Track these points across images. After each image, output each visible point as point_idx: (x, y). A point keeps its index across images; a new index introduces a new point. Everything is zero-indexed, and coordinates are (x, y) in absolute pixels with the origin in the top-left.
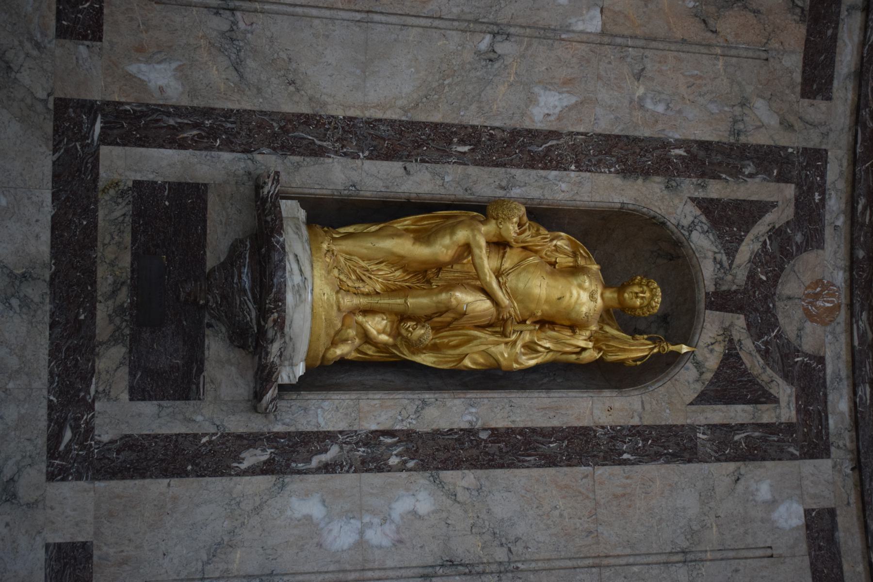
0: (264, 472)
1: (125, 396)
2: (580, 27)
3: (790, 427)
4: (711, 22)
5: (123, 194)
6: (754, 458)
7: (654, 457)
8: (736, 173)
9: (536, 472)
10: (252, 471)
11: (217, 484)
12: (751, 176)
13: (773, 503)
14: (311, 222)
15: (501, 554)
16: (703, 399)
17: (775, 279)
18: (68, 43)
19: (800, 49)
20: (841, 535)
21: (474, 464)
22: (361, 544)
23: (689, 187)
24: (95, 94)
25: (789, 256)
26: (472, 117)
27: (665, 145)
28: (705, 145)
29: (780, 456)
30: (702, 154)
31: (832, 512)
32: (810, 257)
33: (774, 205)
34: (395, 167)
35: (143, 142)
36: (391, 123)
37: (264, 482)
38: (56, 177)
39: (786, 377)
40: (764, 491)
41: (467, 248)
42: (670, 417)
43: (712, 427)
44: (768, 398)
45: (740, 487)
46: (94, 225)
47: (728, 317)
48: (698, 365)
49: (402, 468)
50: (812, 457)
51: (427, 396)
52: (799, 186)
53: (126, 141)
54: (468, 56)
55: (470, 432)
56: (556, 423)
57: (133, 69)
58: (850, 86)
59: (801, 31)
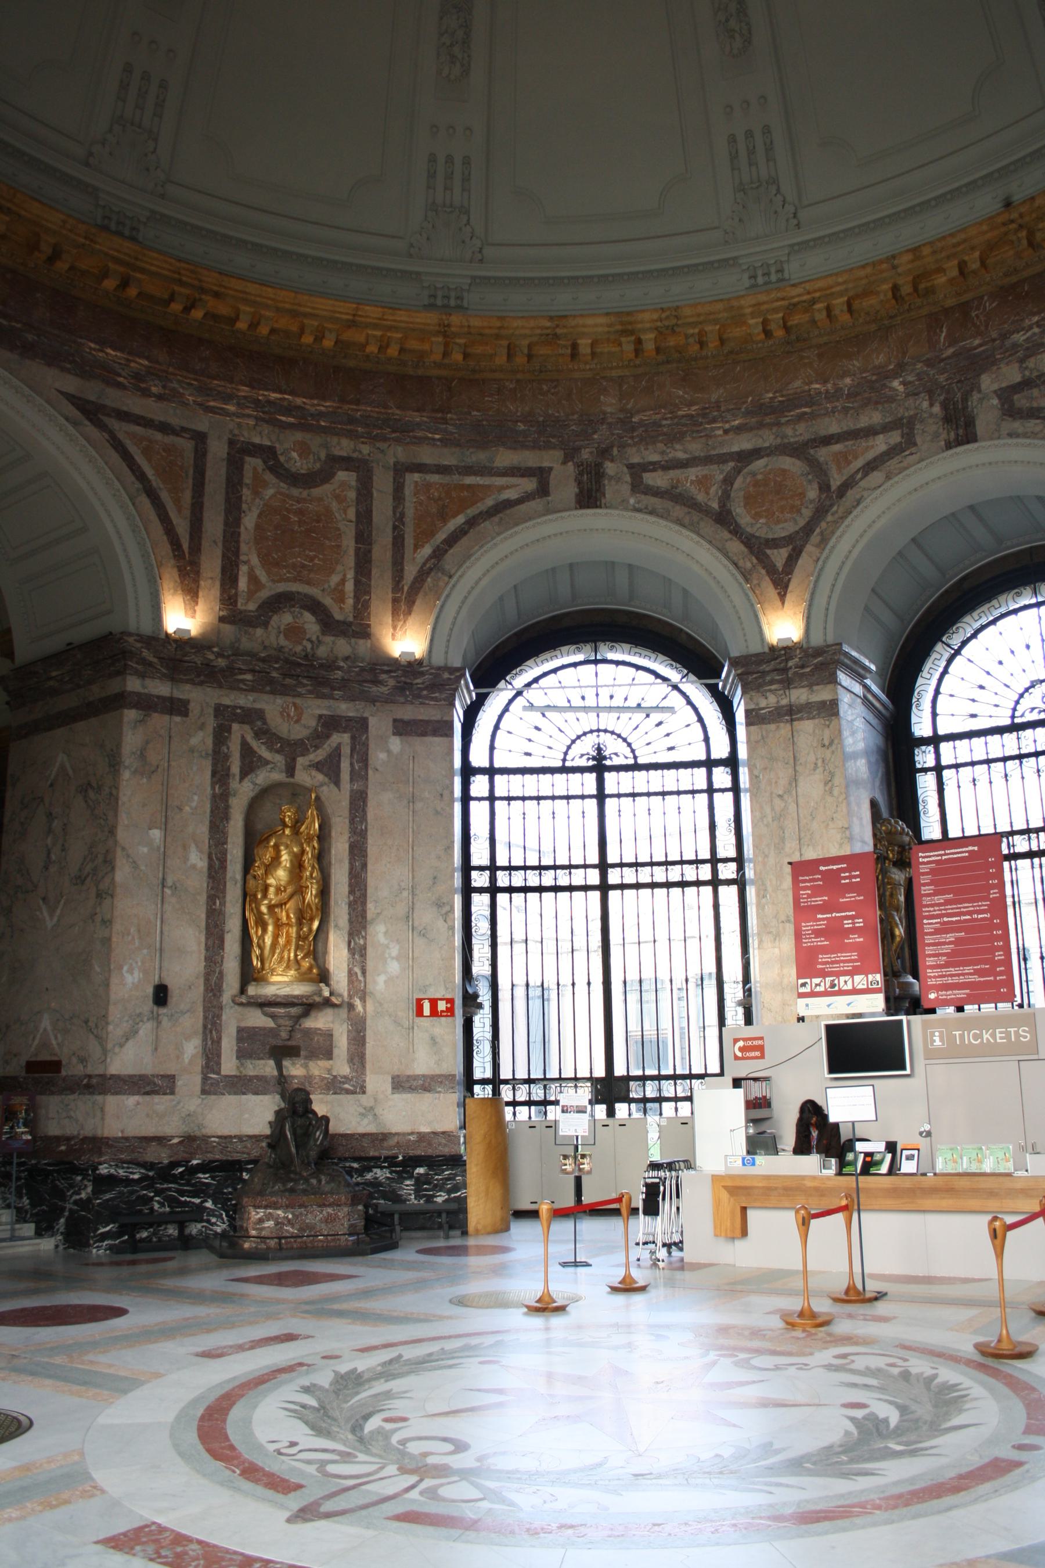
0: (365, 1002)
1: (331, 1062)
2: (158, 841)
3: (353, 738)
4: (153, 769)
5: (242, 1064)
6: (367, 760)
7: (364, 812)
8: (227, 757)
9: (369, 874)
11: (369, 1022)
12: (228, 748)
15: (405, 894)
16: (337, 783)
17: (280, 739)
18: (177, 1090)
20: (406, 717)
21: (364, 903)
22: (397, 958)
23: (234, 784)
24: (198, 1079)
26: (203, 899)
27: (214, 796)
28: (214, 773)
29: (366, 745)
30: (218, 776)
31: (395, 721)
32: (269, 716)
33: (243, 737)
34: (228, 938)
35: (219, 1056)
36: (207, 939)
38: (235, 1093)
39: (328, 737)
40: (383, 756)
42: (345, 803)
43: (352, 780)
44: (338, 748)
46: (256, 1077)
47: (298, 767)
48: (322, 785)
49: (365, 938)
50: (367, 727)
52: (233, 721)
53: (219, 1064)
55: (350, 904)
57: (187, 1061)
59: (155, 715)
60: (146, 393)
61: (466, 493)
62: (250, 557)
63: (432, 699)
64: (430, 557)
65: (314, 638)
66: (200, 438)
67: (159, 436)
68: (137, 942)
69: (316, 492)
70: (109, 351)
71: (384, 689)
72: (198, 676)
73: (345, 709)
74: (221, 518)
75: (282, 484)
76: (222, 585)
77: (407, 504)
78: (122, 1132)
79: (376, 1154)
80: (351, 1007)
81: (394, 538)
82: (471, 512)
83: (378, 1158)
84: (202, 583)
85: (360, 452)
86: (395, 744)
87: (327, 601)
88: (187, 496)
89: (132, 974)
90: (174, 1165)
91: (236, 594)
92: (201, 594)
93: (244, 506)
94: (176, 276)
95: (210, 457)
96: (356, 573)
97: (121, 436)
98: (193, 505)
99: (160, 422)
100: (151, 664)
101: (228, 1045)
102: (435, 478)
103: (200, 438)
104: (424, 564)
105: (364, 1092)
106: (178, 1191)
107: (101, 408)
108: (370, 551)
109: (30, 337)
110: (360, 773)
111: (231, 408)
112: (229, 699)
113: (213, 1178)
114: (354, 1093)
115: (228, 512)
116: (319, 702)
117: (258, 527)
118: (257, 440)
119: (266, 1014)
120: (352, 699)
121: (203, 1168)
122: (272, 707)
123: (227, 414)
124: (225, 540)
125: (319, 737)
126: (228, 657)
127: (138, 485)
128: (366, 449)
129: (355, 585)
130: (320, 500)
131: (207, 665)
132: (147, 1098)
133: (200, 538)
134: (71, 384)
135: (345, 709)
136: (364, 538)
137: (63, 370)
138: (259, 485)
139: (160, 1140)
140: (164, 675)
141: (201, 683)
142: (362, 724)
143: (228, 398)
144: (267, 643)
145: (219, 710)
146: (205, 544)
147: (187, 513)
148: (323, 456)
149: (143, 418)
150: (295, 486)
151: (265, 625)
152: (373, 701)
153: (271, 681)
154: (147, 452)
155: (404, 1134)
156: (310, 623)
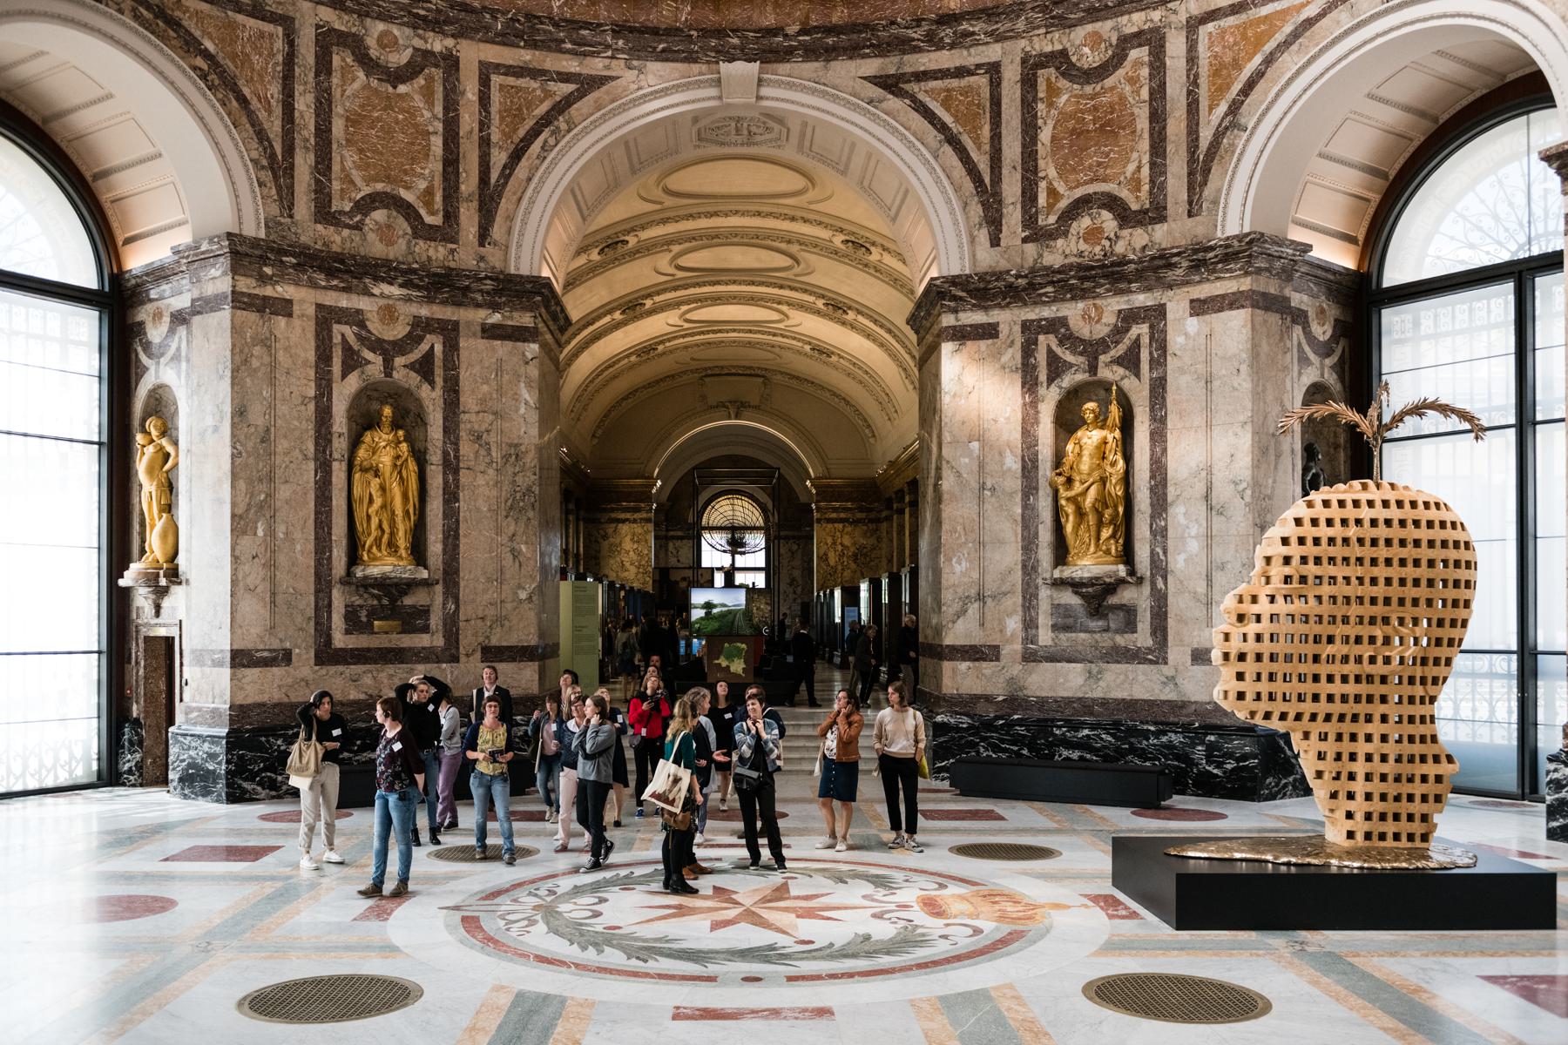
3: (1152, 327)
7: (1164, 398)
8: (1035, 367)
10: (1166, 584)
11: (1170, 599)
13: (1186, 334)
14: (1064, 564)
15: (1204, 474)
16: (1138, 375)
19: (977, 342)
20: (1202, 296)
21: (1165, 486)
24: (1018, 647)
25: (1071, 334)
27: (1024, 405)
29: (1164, 332)
31: (1192, 301)
32: (1071, 323)
33: (1048, 346)
37: (1170, 578)
39: (1128, 331)
41: (1068, 499)
42: (1146, 393)
43: (1151, 369)
45: (1178, 353)
47: (1101, 364)
48: (1122, 379)
49: (1166, 520)
51: (1136, 509)
52: (1039, 333)
53: (1036, 636)
54: (993, 500)
55: (1151, 489)
56: (1148, 449)
60: (939, 46)
61: (1263, 27)
62: (1048, 169)
63: (1231, 271)
64: (1226, 115)
65: (1112, 235)
66: (994, 69)
69: (1109, 82)
71: (1179, 272)
72: (1004, 299)
73: (1142, 299)
75: (1075, 86)
77: (1201, 62)
79: (1176, 720)
80: (1153, 584)
81: (1189, 105)
82: (1269, 47)
83: (1175, 724)
85: (1152, 21)
86: (1193, 324)
87: (1124, 194)
88: (986, 131)
90: (997, 718)
91: (1037, 212)
93: (1040, 122)
95: (1005, 84)
96: (1151, 155)
97: (921, 96)
98: (991, 138)
100: (961, 298)
101: (1044, 620)
102: (1231, 21)
103: (994, 69)
104: (1220, 125)
105: (1166, 663)
106: (998, 739)
108: (1164, 128)
109: (830, 41)
110: (1159, 361)
112: (1031, 314)
113: (1028, 731)
114: (1156, 663)
115: (1025, 132)
116: (1117, 299)
117: (1054, 138)
118: (1048, 49)
119: (1076, 593)
120: (1149, 289)
121: (1020, 722)
122: (1073, 311)
125: (1119, 332)
126: (1026, 276)
128: (1156, 15)
129: (1151, 169)
130: (1112, 88)
131: (1010, 286)
132: (977, 664)
133: (1000, 168)
134: (872, 66)
135: (1142, 299)
136: (1158, 117)
138: (1053, 91)
139: (988, 699)
140: (974, 305)
142: (1160, 311)
144: (1067, 252)
145: (1026, 326)
146: (1005, 171)
147: (987, 147)
148: (1114, 42)
149: (940, 70)
150: (1088, 83)
151: (1066, 234)
152: (1170, 287)
153: (1072, 288)
154: (946, 105)
155: (1202, 704)
156: (1108, 221)
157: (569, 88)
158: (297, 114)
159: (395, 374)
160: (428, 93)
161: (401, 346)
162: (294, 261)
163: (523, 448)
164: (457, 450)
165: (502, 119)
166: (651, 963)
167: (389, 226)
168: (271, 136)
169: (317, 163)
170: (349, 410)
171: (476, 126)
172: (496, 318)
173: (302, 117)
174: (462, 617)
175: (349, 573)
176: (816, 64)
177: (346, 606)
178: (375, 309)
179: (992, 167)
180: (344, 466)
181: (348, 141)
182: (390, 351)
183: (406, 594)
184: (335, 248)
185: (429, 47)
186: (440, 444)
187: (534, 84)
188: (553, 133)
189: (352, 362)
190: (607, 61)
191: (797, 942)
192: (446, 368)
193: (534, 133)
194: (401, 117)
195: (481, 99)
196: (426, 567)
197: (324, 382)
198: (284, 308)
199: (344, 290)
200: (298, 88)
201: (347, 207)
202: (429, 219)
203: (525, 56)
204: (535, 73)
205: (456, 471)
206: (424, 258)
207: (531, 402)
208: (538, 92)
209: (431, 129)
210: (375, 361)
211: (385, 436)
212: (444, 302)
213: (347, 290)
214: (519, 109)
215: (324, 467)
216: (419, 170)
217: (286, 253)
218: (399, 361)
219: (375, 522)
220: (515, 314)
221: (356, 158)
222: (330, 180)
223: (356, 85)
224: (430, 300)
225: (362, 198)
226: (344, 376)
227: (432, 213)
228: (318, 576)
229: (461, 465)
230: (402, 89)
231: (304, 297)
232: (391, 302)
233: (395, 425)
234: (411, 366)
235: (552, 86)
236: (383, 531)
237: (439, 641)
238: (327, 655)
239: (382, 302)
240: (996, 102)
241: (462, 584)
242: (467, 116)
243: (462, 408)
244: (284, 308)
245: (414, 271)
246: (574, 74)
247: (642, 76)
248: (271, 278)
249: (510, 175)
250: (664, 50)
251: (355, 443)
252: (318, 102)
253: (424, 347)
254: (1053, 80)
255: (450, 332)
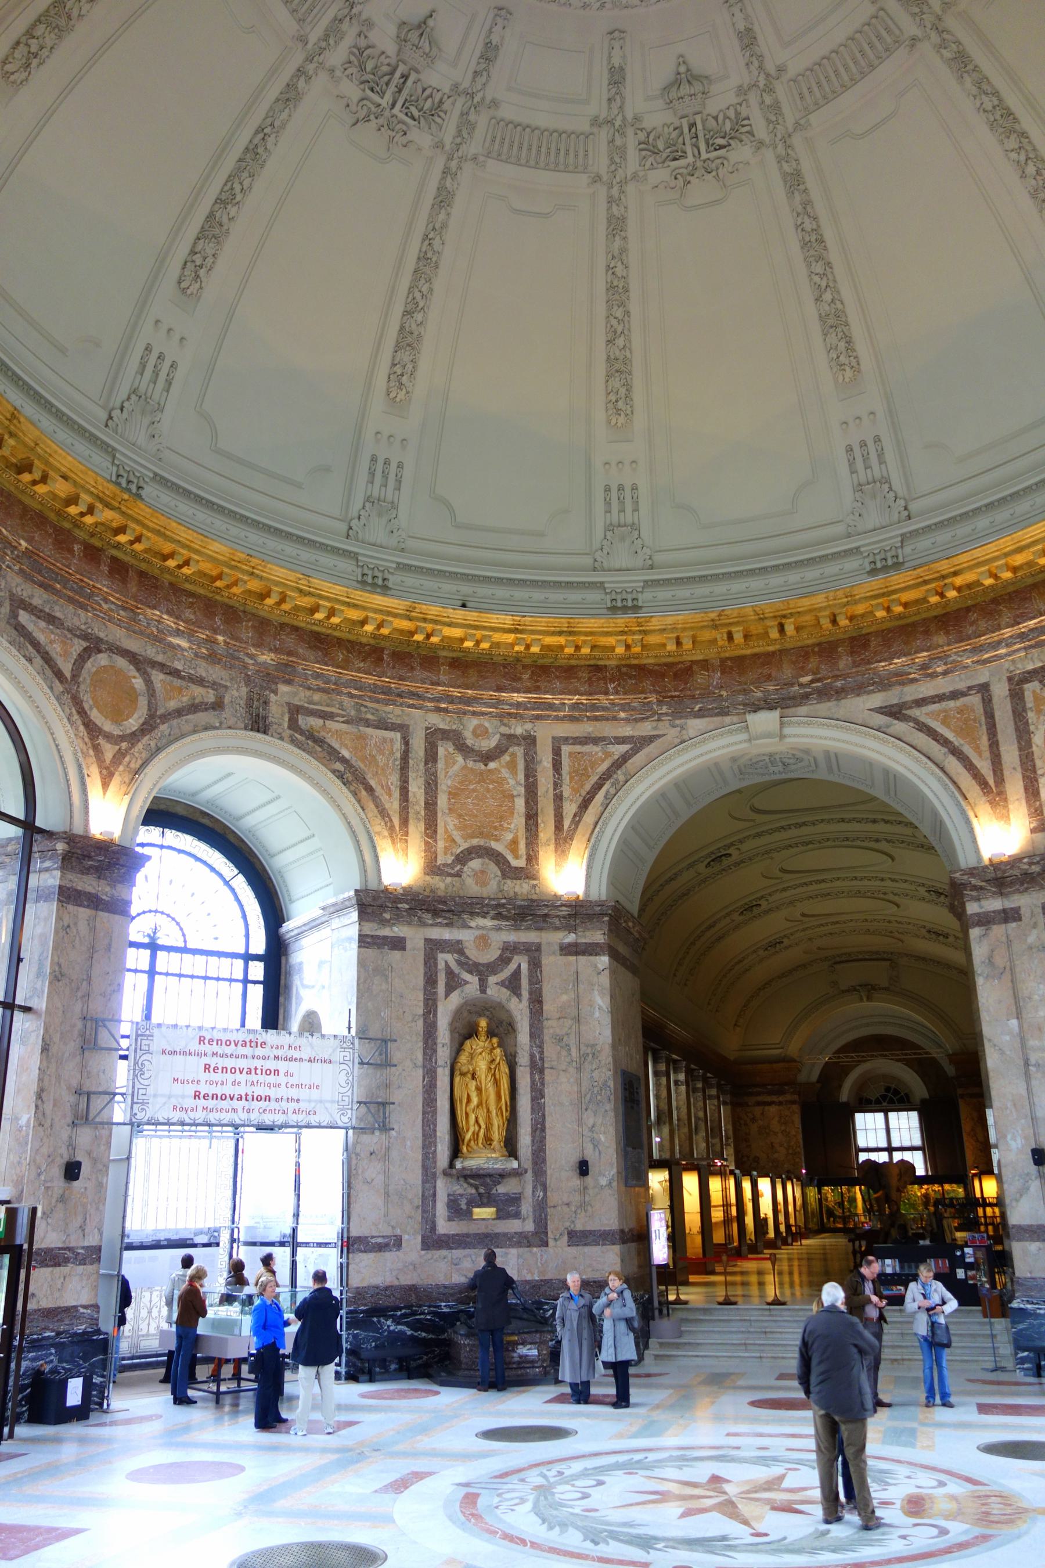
58: (1012, 899)
59: (994, 927)
60: (934, 676)
66: (984, 689)
67: (951, 704)
68: (1014, 1114)
70: (896, 661)
72: (1022, 884)
74: (1015, 746)
76: (1028, 801)
78: (1031, 1273)
84: (1011, 807)
88: (984, 741)
89: (1015, 1140)
92: (1011, 816)
93: (1032, 728)
94: (920, 580)
95: (995, 700)
98: (990, 746)
99: (951, 692)
100: (981, 888)
103: (984, 689)
107: (903, 706)
109: (839, 684)
111: (1003, 651)
115: (1019, 738)
118: (1030, 667)
123: (1000, 657)
124: (1022, 764)
126: (1038, 863)
127: (944, 750)
133: (1002, 770)
134: (878, 699)
137: (869, 693)
140: (994, 893)
141: (1026, 890)
143: (996, 645)
146: (1006, 773)
149: (937, 696)
154: (945, 722)
157: (624, 748)
158: (410, 794)
159: (489, 991)
160: (512, 766)
161: (492, 968)
162: (407, 906)
163: (598, 1048)
164: (542, 1053)
165: (571, 778)
166: (602, 1547)
167: (483, 872)
168: (391, 813)
169: (426, 829)
170: (451, 1024)
171: (551, 787)
172: (571, 938)
173: (415, 796)
174: (550, 1203)
175: (451, 1165)
176: (829, 704)
177: (449, 1195)
178: (472, 938)
179: (994, 770)
180: (447, 1071)
181: (450, 809)
182: (482, 971)
183: (499, 1183)
184: (441, 893)
185: (512, 732)
186: (528, 1048)
187: (596, 749)
188: (613, 784)
189: (453, 983)
190: (654, 724)
191: (752, 1535)
192: (531, 983)
193: (598, 786)
194: (491, 786)
195: (554, 765)
196: (516, 1158)
197: (430, 1002)
198: (398, 944)
199: (447, 925)
200: (412, 775)
201: (450, 859)
202: (515, 863)
203: (587, 728)
204: (595, 741)
205: (541, 1071)
206: (512, 894)
207: (604, 1007)
208: (600, 754)
209: (515, 793)
210: (473, 980)
211: (481, 1044)
212: (528, 929)
213: (449, 925)
214: (585, 769)
215: (430, 1074)
216: (506, 825)
217: (401, 901)
218: (492, 980)
219: (472, 1117)
220: (588, 933)
221: (456, 822)
222: (436, 841)
223: (456, 768)
224: (516, 928)
225: (462, 852)
226: (447, 995)
227: (517, 857)
228: (425, 1168)
229: (546, 1065)
230: (492, 765)
231: (415, 935)
232: (484, 932)
233: (491, 1034)
234: (502, 984)
235: (611, 748)
236: (480, 1127)
237: (529, 1226)
238: (432, 1241)
239: (478, 933)
240: (990, 716)
241: (549, 1172)
242: (543, 780)
243: (545, 1016)
244: (398, 944)
245: (503, 906)
246: (628, 737)
247: (684, 732)
248: (388, 921)
249: (579, 821)
250: (700, 710)
251: (458, 1050)
252: (428, 784)
253: (513, 966)
254: (1038, 691)
255: (533, 952)
